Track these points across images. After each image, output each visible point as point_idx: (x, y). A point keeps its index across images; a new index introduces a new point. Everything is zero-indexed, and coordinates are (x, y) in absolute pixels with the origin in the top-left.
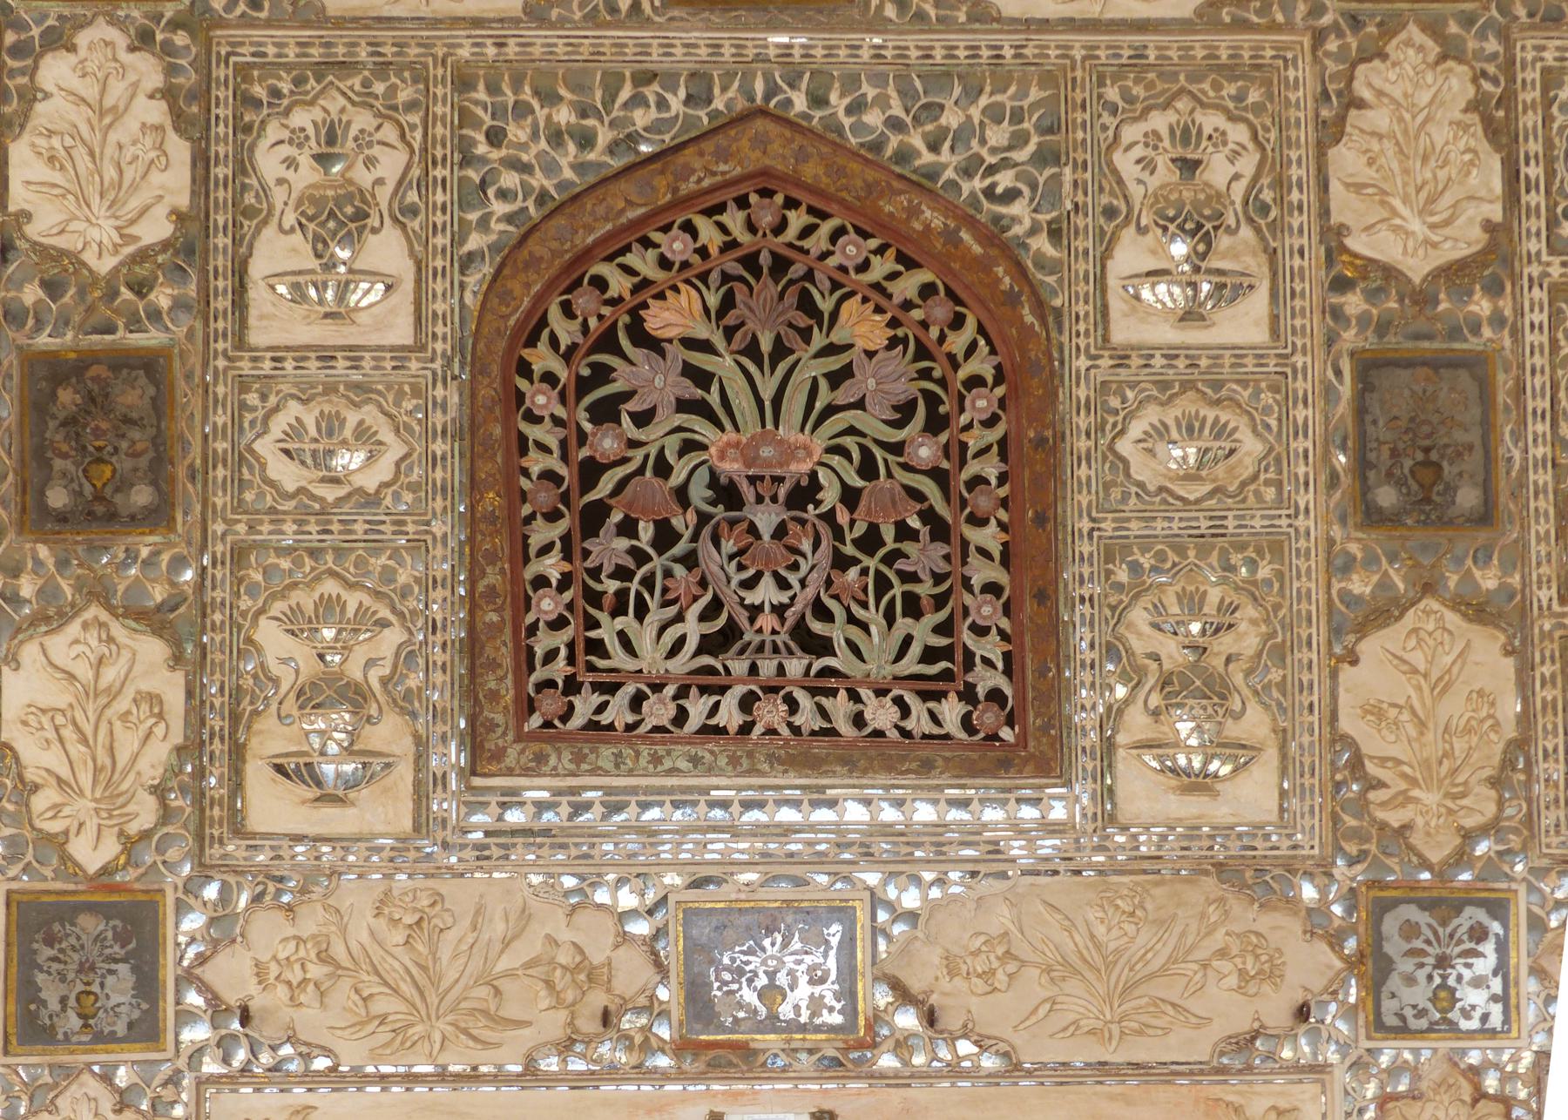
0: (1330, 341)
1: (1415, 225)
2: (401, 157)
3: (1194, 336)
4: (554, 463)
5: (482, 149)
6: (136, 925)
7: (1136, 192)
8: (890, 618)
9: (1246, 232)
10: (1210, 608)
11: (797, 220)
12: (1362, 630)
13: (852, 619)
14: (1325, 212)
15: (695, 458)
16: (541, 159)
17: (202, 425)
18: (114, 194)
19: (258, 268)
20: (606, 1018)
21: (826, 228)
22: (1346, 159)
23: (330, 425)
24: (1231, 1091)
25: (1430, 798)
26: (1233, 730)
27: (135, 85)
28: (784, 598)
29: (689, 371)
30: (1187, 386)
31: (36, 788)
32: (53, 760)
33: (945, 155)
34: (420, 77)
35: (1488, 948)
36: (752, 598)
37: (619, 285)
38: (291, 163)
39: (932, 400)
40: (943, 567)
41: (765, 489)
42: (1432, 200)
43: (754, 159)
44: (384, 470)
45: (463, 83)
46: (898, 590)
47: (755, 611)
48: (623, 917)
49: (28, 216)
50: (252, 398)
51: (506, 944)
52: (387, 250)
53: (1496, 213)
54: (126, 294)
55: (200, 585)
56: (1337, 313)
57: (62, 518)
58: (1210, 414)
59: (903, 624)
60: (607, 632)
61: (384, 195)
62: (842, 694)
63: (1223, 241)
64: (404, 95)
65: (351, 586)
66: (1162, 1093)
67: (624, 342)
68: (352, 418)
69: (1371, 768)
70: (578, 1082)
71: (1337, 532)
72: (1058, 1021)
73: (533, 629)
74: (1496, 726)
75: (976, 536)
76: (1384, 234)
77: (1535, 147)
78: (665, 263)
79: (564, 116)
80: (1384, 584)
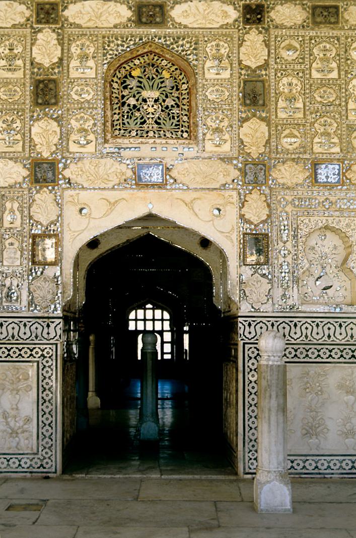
0: (240, 78)
1: (253, 60)
2: (94, 49)
3: (218, 77)
4: (117, 95)
5: (106, 47)
6: (53, 165)
7: (209, 54)
8: (170, 119)
9: (227, 60)
10: (220, 118)
11: (156, 58)
12: (243, 122)
13: (164, 120)
14: (239, 58)
15: (140, 94)
16: (115, 48)
17: (63, 90)
18: (49, 55)
19: (71, 66)
20: (125, 180)
21: (161, 59)
22: (243, 49)
23: (82, 90)
24: (223, 192)
25: (254, 148)
26: (224, 138)
27: (52, 38)
28: (153, 116)
29: (139, 81)
30: (217, 84)
31: (37, 145)
32: (39, 140)
33: (179, 49)
34: (97, 36)
35: (263, 171)
36: (148, 116)
37: (128, 68)
38: (76, 50)
39: (177, 86)
40: (178, 112)
41: (151, 100)
42: (256, 56)
43: (150, 49)
44: (91, 97)
45: (104, 37)
46: (171, 115)
47: (148, 118)
48: (128, 165)
49: (35, 58)
50: (70, 86)
51: (110, 169)
52: (91, 63)
53: (266, 58)
54: (51, 70)
55: (62, 115)
56: (241, 73)
57: (41, 104)
58: (221, 89)
59: (172, 120)
60: (125, 121)
61: (91, 54)
62: (162, 132)
63: (223, 62)
64: (94, 39)
65: (85, 114)
66: (211, 193)
67: (128, 76)
68: (86, 89)
69: (245, 143)
70: (121, 190)
71: (240, 107)
72: (195, 182)
73: (114, 121)
74: (265, 137)
75: (184, 107)
76: (248, 61)
77: (273, 48)
78: (135, 65)
79: (119, 42)
80: (247, 115)
